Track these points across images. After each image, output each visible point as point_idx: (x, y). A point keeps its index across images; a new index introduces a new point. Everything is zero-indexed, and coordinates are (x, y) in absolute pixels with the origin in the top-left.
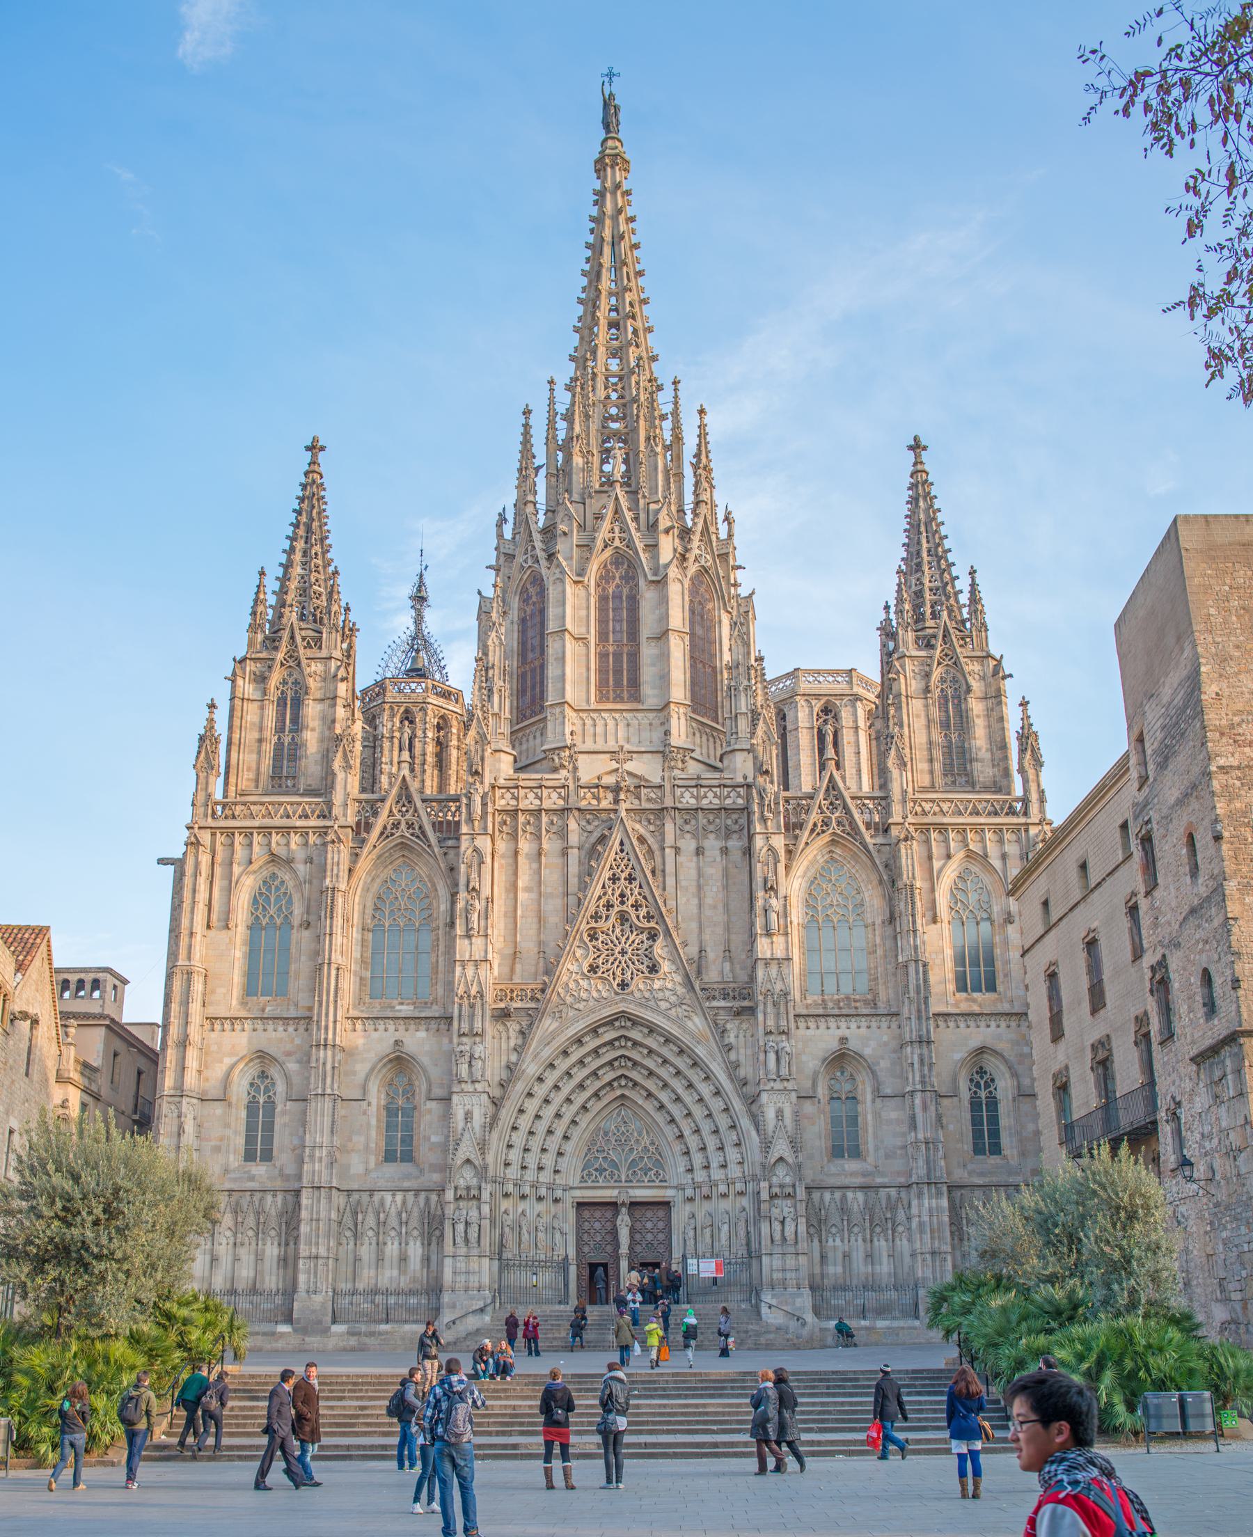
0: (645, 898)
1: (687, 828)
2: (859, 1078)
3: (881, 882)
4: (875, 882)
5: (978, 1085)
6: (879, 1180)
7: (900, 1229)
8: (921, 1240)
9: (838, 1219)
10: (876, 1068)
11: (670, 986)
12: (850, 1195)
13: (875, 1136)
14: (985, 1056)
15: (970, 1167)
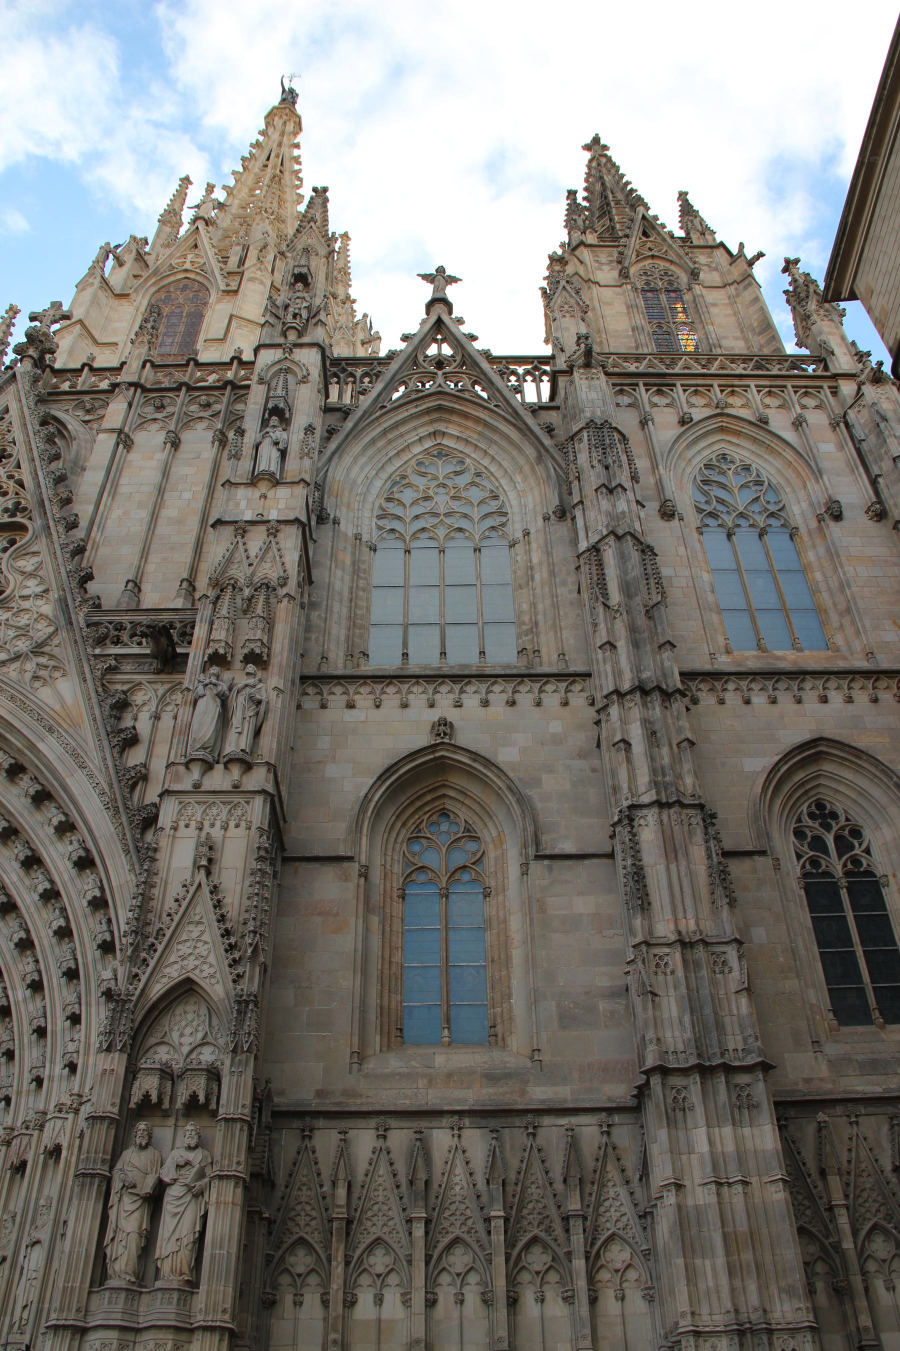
0: (21, 484)
1: (159, 416)
2: (488, 834)
3: (540, 459)
4: (527, 468)
5: (818, 844)
6: (541, 1093)
7: (618, 1255)
8: (692, 1276)
9: (398, 1222)
10: (529, 792)
11: (23, 620)
12: (441, 1139)
13: (531, 963)
14: (827, 767)
15: (831, 1049)
